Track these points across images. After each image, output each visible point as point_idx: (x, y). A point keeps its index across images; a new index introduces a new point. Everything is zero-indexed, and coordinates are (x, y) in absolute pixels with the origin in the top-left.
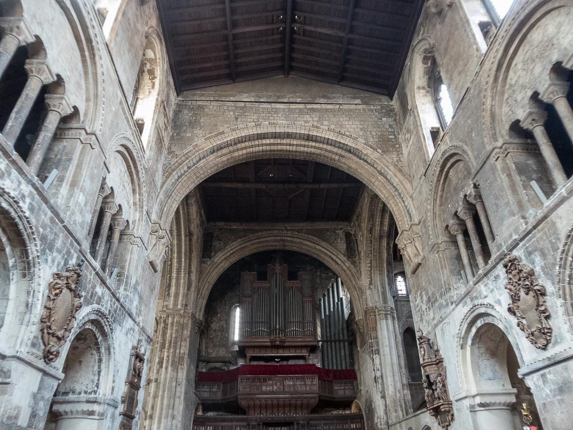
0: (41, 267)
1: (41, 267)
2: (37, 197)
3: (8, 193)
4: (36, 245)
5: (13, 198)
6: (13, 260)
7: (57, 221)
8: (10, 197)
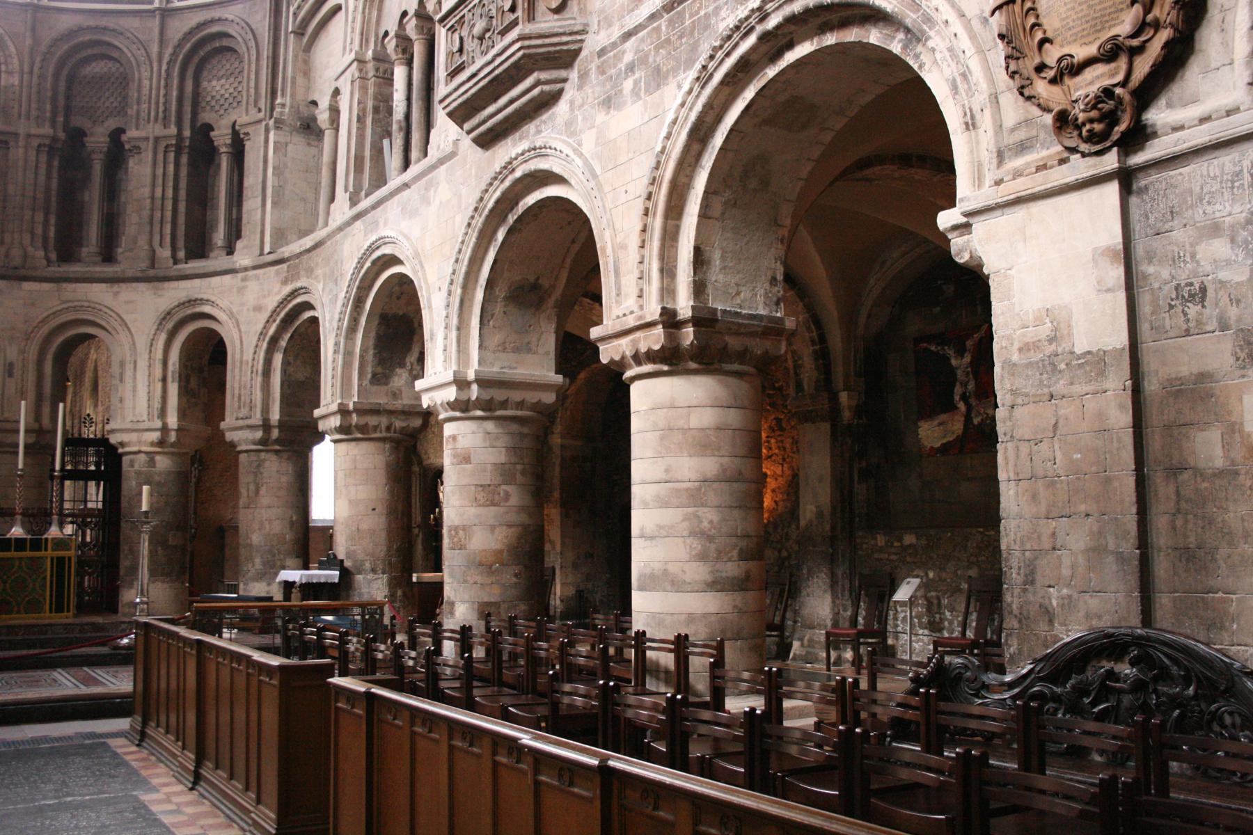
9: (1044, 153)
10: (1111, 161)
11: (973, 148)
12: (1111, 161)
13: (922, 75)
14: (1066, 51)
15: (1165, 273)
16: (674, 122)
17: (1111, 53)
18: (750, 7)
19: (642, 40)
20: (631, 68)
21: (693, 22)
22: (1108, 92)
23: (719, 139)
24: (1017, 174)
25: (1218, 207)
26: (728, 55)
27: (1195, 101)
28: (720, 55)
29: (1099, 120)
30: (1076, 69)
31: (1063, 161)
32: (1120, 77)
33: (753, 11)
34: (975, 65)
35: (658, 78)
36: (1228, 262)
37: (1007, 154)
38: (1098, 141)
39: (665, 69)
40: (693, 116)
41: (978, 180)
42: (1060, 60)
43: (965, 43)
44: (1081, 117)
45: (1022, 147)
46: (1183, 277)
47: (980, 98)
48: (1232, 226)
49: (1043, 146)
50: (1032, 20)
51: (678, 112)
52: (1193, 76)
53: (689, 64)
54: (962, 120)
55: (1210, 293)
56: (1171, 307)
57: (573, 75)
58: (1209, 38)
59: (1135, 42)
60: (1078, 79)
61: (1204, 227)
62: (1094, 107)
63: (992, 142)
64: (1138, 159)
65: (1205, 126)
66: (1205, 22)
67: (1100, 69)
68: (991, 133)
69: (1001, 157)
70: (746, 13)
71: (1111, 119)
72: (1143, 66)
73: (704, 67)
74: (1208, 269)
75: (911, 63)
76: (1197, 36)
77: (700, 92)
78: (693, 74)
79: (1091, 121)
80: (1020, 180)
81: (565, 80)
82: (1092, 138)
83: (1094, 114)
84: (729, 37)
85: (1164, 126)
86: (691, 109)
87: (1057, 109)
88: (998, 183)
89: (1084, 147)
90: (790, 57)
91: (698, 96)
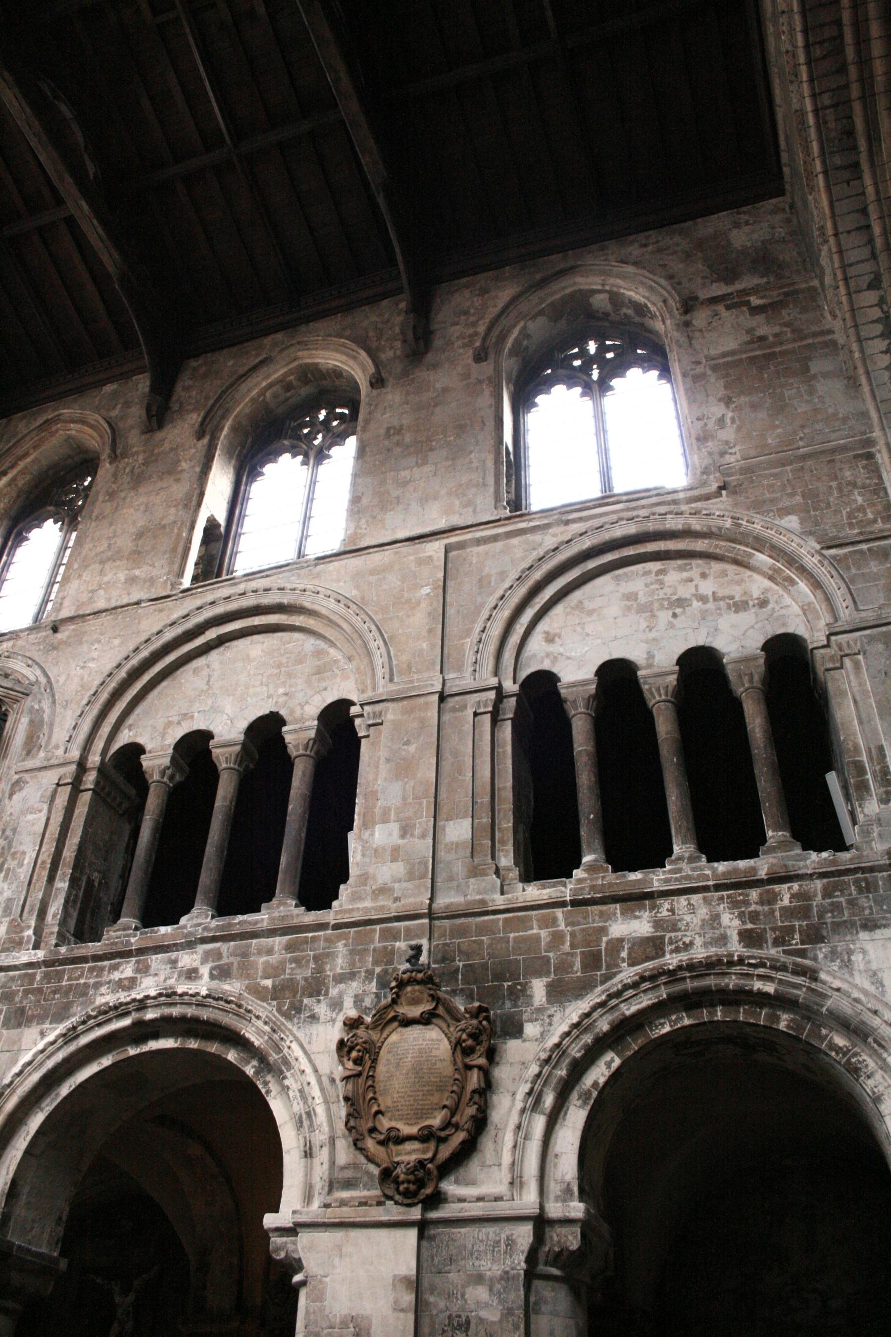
0: (288, 1043)
1: (288, 1043)
2: (224, 947)
3: (147, 997)
4: (258, 1017)
5: (160, 995)
6: (255, 1063)
7: (310, 935)
8: (154, 998)
9: (366, 1193)
10: (416, 1213)
11: (308, 1172)
12: (416, 1213)
13: (268, 1099)
14: (394, 1124)
15: (442, 1304)
16: (29, 1063)
17: (426, 1136)
18: (133, 996)
19: (12, 979)
21: (71, 985)
22: (421, 1164)
23: (65, 1090)
24: (343, 1203)
25: (482, 1262)
26: (99, 1025)
27: (473, 1183)
28: (91, 1022)
29: (414, 1184)
30: (401, 1140)
31: (380, 1204)
32: (429, 1155)
33: (134, 1000)
34: (320, 1110)
36: (487, 1305)
37: (336, 1185)
38: (409, 1197)
39: (30, 1013)
40: (50, 1064)
41: (308, 1198)
42: (390, 1129)
43: (316, 1092)
44: (402, 1177)
45: (349, 1184)
46: (454, 1310)
47: (321, 1136)
48: (491, 1279)
49: (365, 1187)
50: (371, 1095)
51: (35, 1056)
52: (474, 1166)
53: (58, 1018)
54: (302, 1148)
55: (473, 1326)
56: (444, 1331)
58: (487, 1144)
59: (443, 1134)
60: (400, 1147)
61: (472, 1275)
62: (412, 1173)
63: (327, 1173)
64: (433, 1215)
65: (481, 1204)
66: (484, 1133)
67: (416, 1145)
68: (326, 1166)
69: (331, 1186)
70: (128, 999)
71: (421, 1184)
72: (445, 1152)
73: (74, 1028)
74: (473, 1307)
75: (260, 1087)
76: (479, 1140)
77: (61, 1047)
78: (61, 1028)
79: (409, 1182)
80: (345, 1209)
82: (406, 1194)
83: (411, 1177)
84: (106, 1012)
85: (454, 1196)
86: (49, 1057)
87: (384, 1166)
88: (327, 1206)
89: (397, 1197)
90: (154, 1045)
91: (59, 1049)
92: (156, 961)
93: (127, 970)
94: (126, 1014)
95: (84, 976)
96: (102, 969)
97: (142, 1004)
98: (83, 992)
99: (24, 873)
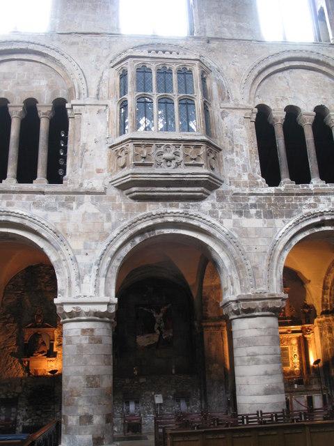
3: (325, 211)
20: (254, 206)
35: (269, 215)
53: (289, 215)
57: (214, 194)
78: (293, 220)
81: (209, 195)
92: (322, 198)
93: (311, 200)
94: (316, 217)
95: (294, 201)
96: (300, 199)
97: (322, 214)
98: (295, 207)
99: (246, 153)
